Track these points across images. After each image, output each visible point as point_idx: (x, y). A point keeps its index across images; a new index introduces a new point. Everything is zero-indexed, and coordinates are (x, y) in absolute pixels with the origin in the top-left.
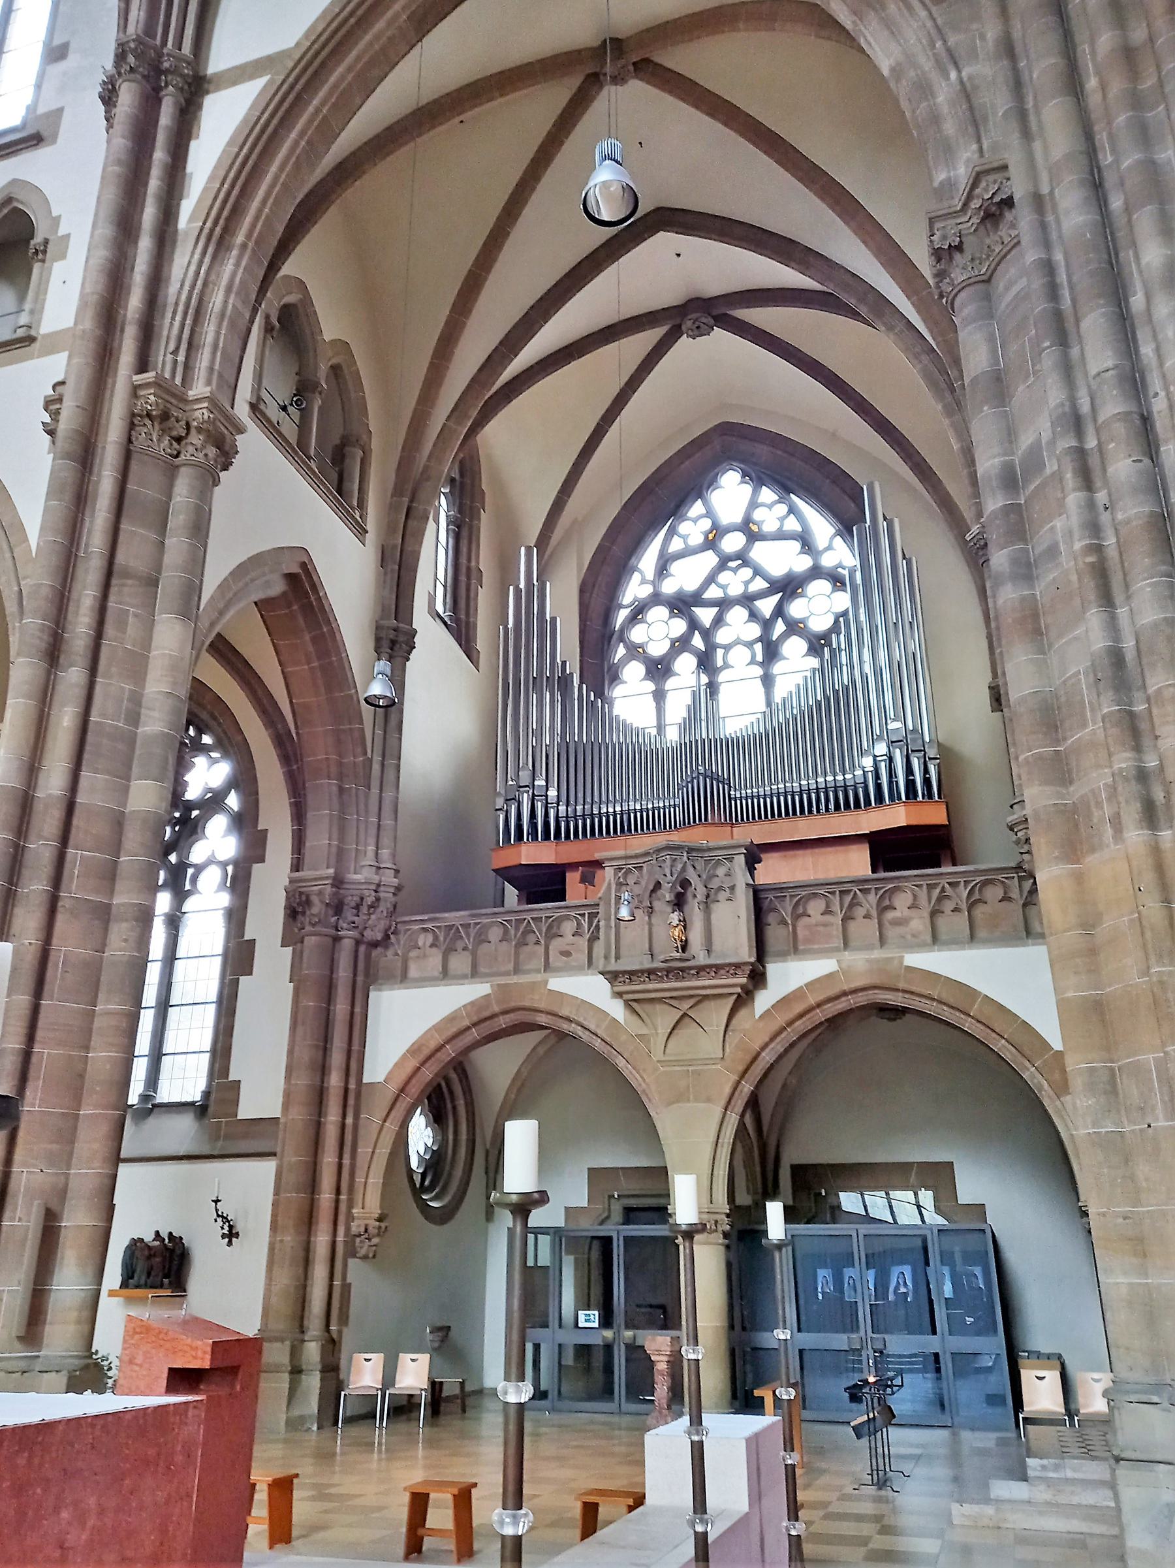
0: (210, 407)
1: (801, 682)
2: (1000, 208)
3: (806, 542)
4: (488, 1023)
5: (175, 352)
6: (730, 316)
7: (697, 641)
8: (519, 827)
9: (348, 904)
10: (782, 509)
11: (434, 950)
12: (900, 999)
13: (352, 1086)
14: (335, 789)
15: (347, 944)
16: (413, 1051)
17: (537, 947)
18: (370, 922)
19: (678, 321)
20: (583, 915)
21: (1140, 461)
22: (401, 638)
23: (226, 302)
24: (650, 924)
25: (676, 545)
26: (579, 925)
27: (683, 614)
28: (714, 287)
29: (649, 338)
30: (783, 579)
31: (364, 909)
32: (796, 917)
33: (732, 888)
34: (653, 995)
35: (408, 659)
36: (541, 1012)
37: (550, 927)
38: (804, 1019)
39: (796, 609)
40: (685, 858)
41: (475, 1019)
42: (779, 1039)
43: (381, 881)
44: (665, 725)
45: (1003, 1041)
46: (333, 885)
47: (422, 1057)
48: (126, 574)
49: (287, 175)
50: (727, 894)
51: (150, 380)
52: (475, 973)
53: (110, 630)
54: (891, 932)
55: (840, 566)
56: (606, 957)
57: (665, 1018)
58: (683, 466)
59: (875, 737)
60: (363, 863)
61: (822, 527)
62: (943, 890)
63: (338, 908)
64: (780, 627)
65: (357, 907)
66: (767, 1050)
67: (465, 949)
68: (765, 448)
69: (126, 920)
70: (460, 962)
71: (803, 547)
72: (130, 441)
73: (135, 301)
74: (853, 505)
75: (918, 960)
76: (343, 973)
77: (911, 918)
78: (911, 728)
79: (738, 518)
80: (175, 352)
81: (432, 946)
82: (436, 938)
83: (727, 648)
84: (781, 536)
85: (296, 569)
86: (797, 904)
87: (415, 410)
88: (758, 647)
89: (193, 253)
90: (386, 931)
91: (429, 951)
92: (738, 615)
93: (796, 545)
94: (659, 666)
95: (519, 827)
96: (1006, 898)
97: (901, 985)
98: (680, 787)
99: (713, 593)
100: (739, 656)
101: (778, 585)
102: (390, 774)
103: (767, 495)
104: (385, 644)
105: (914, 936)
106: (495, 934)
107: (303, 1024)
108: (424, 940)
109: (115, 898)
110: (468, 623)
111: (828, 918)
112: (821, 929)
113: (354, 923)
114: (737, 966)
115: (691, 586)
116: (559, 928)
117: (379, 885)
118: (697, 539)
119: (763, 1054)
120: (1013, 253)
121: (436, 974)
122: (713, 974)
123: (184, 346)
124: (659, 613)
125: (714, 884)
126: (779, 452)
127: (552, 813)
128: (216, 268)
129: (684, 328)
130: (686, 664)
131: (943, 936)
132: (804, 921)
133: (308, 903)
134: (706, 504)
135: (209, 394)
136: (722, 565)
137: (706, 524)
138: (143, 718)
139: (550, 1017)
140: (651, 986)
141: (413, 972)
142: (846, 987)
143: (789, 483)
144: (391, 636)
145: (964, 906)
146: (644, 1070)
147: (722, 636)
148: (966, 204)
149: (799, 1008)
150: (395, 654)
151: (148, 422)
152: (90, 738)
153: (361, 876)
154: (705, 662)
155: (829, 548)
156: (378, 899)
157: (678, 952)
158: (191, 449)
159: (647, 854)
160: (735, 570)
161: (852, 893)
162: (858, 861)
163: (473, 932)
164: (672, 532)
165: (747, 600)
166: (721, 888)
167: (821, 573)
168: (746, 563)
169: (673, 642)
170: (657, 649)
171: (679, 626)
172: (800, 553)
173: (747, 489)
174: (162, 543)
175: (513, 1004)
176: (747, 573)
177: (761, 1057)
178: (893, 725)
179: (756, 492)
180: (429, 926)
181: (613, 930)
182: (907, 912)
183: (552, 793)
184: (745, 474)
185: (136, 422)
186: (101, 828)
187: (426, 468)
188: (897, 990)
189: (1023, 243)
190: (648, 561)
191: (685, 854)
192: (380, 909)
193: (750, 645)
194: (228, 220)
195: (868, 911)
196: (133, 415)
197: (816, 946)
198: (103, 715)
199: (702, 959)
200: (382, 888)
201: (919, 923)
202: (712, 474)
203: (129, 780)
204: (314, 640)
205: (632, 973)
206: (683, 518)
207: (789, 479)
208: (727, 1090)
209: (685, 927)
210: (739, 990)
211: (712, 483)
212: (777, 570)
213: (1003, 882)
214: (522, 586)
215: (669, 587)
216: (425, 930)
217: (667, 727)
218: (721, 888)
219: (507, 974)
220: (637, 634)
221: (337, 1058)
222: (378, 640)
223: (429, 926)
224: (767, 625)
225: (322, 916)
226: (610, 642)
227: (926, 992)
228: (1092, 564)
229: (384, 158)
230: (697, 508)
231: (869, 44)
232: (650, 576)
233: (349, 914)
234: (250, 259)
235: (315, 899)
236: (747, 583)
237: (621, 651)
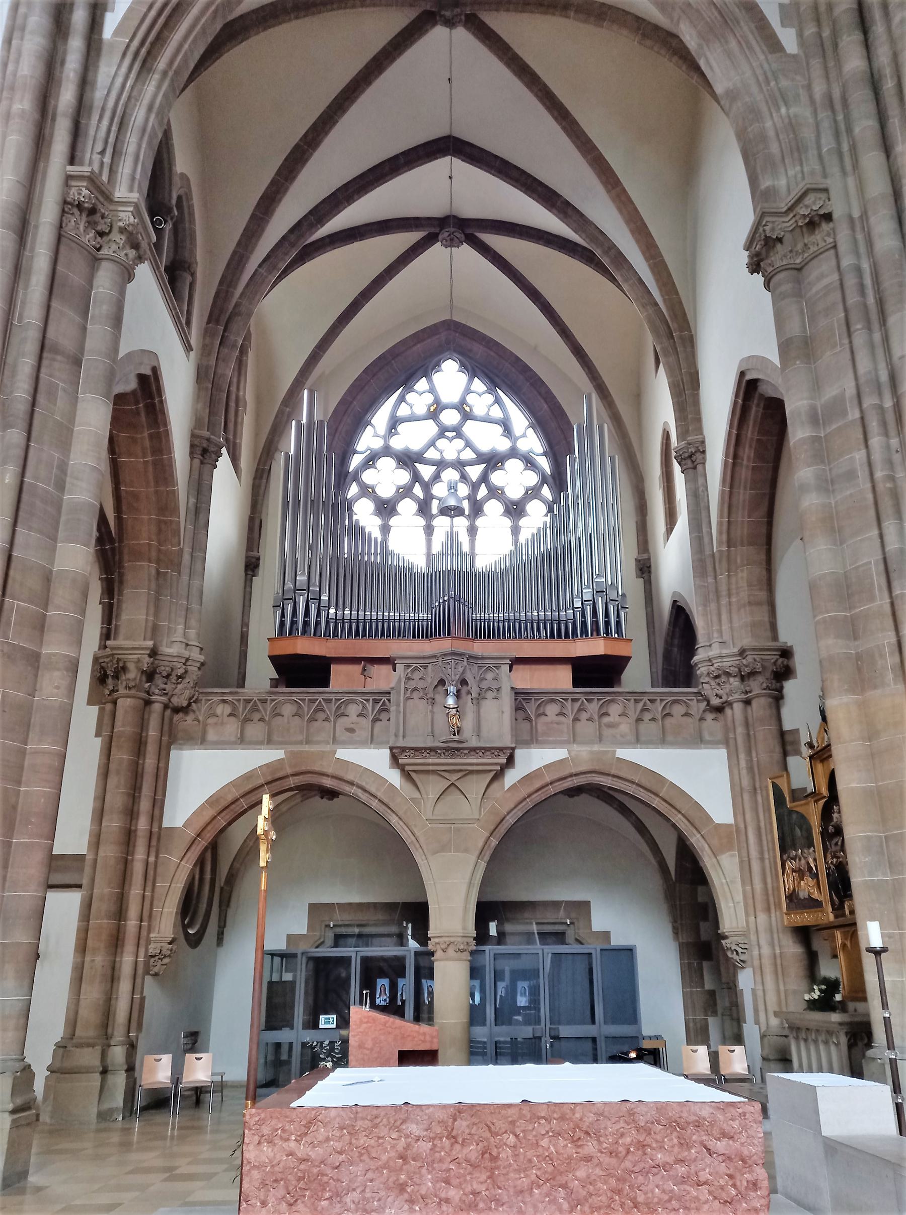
0: (134, 212)
1: (530, 537)
2: (820, 219)
3: (507, 430)
4: (278, 783)
5: (102, 153)
6: (476, 237)
7: (418, 490)
8: (293, 623)
9: (160, 673)
10: (490, 398)
11: (232, 719)
12: (609, 782)
13: (155, 830)
14: (153, 572)
15: (157, 707)
16: (211, 802)
17: (326, 723)
18: (176, 691)
19: (437, 230)
20: (566, 700)
22: (212, 449)
23: (147, 120)
24: (432, 712)
25: (404, 410)
26: (364, 707)
27: (408, 467)
28: (469, 210)
29: (414, 237)
30: (489, 453)
31: (173, 678)
32: (539, 716)
34: (431, 768)
35: (215, 467)
36: (328, 776)
37: (339, 707)
38: (540, 792)
39: (496, 478)
40: (465, 663)
41: (269, 778)
42: (520, 806)
43: (190, 656)
45: (680, 816)
46: (150, 656)
47: (220, 807)
48: (56, 350)
49: (206, 21)
50: (494, 694)
51: (86, 174)
52: (269, 741)
53: (42, 399)
54: (607, 732)
56: (396, 736)
57: (433, 787)
58: (415, 348)
59: (583, 587)
60: (174, 639)
61: (519, 420)
62: (645, 704)
63: (150, 675)
64: (483, 491)
65: (168, 676)
66: (510, 815)
67: (261, 720)
68: (481, 347)
69: (58, 670)
70: (254, 730)
71: (504, 431)
72: (61, 227)
73: (66, 96)
74: (546, 406)
75: (623, 753)
76: (153, 732)
77: (620, 723)
78: (610, 583)
79: (455, 399)
80: (102, 153)
81: (230, 715)
82: (235, 708)
84: (487, 420)
85: (148, 372)
86: (539, 705)
87: (235, 252)
89: (119, 66)
90: (191, 699)
91: (226, 719)
92: (450, 475)
93: (499, 429)
95: (293, 623)
96: (687, 714)
97: (613, 772)
99: (432, 454)
101: (484, 457)
102: (198, 566)
103: (478, 385)
104: (199, 451)
105: (622, 736)
106: (288, 710)
107: (118, 772)
108: (219, 710)
109: (44, 647)
111: (562, 718)
112: (555, 725)
113: (165, 690)
114: (501, 749)
115: (416, 446)
116: (345, 708)
117: (187, 660)
118: (421, 410)
119: (508, 817)
121: (233, 739)
122: (481, 754)
124: (386, 464)
125: (484, 685)
126: (492, 353)
127: (323, 614)
128: (139, 86)
129: (440, 237)
130: (407, 507)
131: (643, 739)
132: (543, 718)
133: (124, 669)
134: (430, 381)
135: (135, 200)
137: (430, 398)
138: (67, 486)
139: (334, 780)
140: (430, 761)
141: (211, 736)
142: (574, 771)
143: (497, 380)
144: (205, 445)
145: (659, 717)
146: (415, 826)
148: (791, 209)
149: (538, 785)
150: (205, 461)
151: (76, 211)
152: (25, 496)
153: (172, 649)
154: (424, 509)
155: (524, 435)
156: (186, 672)
157: (454, 735)
158: (114, 247)
159: (434, 657)
160: (451, 440)
161: (580, 702)
162: (563, 678)
163: (269, 707)
164: (402, 399)
165: (460, 465)
166: (489, 689)
167: (517, 454)
168: (459, 435)
169: (398, 488)
170: (386, 491)
173: (463, 378)
174: (84, 329)
175: (303, 768)
176: (459, 443)
177: (506, 819)
179: (471, 380)
180: (229, 698)
181: (402, 714)
182: (617, 719)
183: (325, 598)
184: (462, 365)
185: (66, 209)
186: (34, 583)
187: (237, 305)
188: (608, 775)
190: (381, 417)
191: (465, 660)
192: (187, 680)
194: (153, 44)
195: (591, 714)
196: (65, 202)
197: (551, 739)
198: (36, 478)
199: (474, 743)
200: (189, 663)
201: (625, 727)
202: (436, 359)
203: (55, 539)
204: (151, 437)
205: (417, 750)
206: (410, 389)
207: (497, 376)
208: (480, 844)
211: (437, 366)
212: (485, 447)
213: (685, 702)
214: (304, 421)
215: (397, 443)
216: (224, 701)
218: (489, 689)
219: (301, 743)
220: (368, 476)
221: (145, 805)
222: (192, 446)
223: (229, 698)
224: (475, 487)
225: (138, 681)
227: (629, 777)
228: (890, 489)
229: (265, 29)
230: (422, 384)
231: (711, 67)
233: (159, 681)
234: (169, 86)
235: (131, 666)
237: (354, 490)
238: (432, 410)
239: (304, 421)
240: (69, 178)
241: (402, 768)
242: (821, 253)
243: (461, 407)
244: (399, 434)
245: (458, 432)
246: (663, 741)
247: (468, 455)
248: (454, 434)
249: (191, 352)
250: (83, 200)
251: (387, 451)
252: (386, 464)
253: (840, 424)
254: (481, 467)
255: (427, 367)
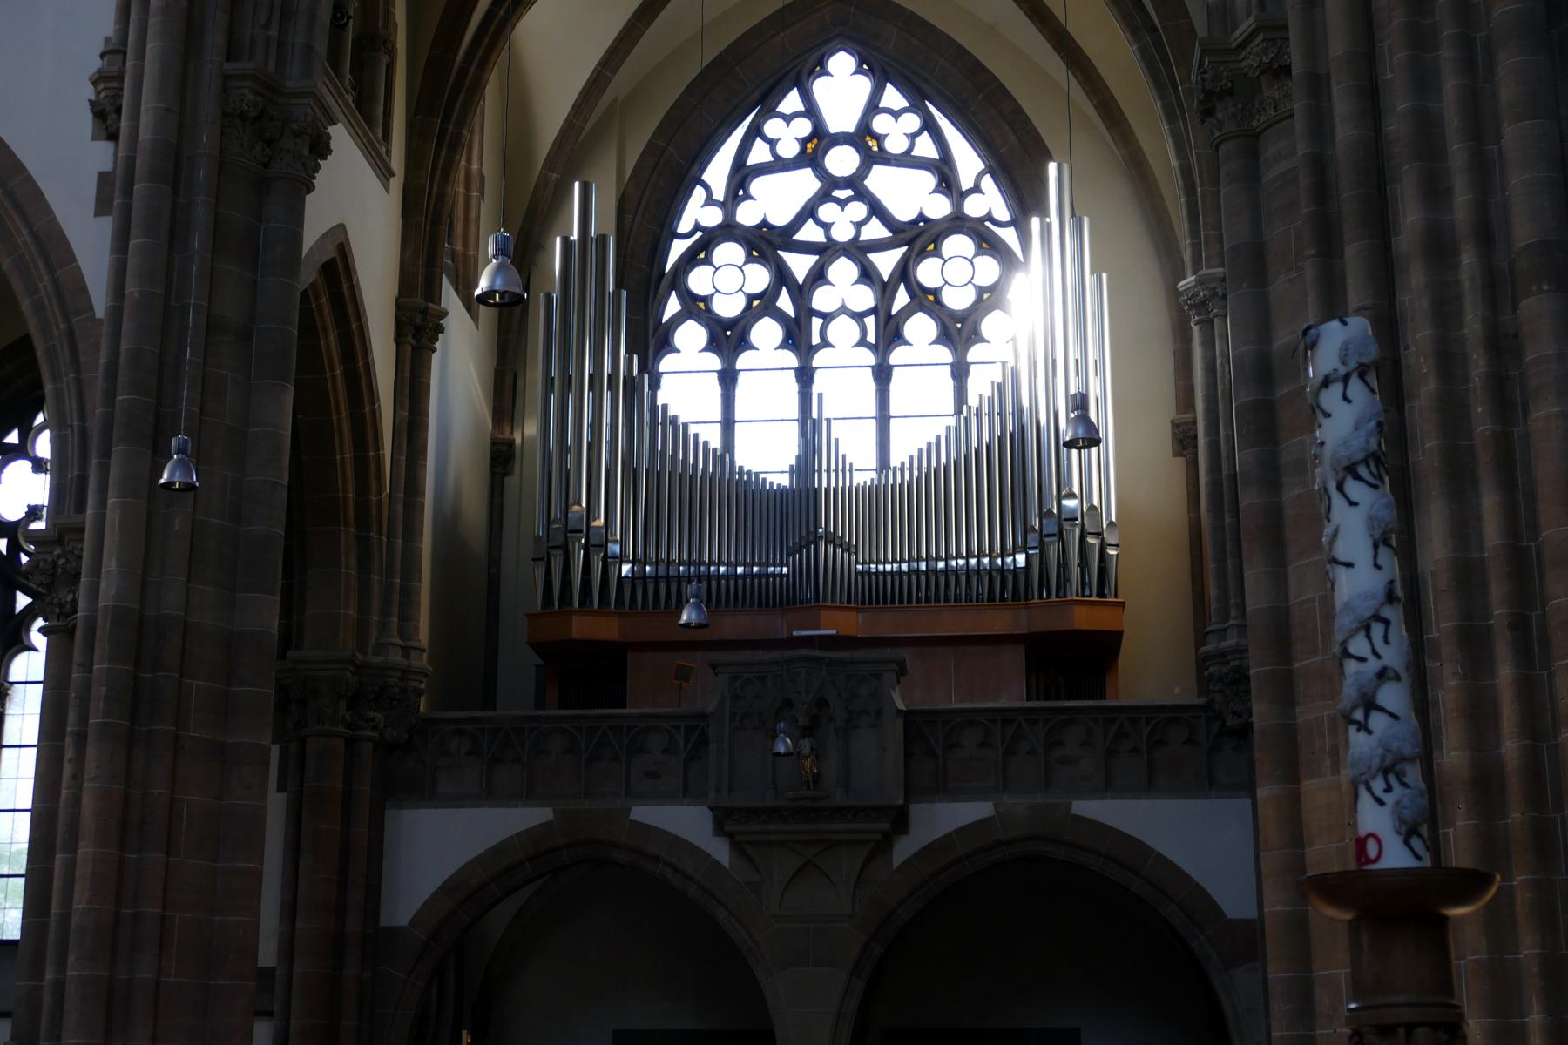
7: (785, 302)
10: (912, 122)
21: (1389, 411)
33: (879, 713)
39: (928, 272)
44: (734, 422)
52: (527, 795)
55: (989, 217)
61: (968, 161)
64: (902, 298)
71: (939, 185)
79: (850, 127)
83: (827, 317)
84: (907, 160)
88: (870, 321)
92: (843, 270)
93: (928, 179)
94: (729, 333)
98: (791, 550)
99: (810, 233)
100: (843, 332)
103: (893, 97)
110: (466, 257)
115: (780, 219)
118: (789, 150)
120: (1285, 122)
123: (276, 17)
124: (729, 252)
130: (766, 332)
136: (824, 196)
137: (804, 127)
143: (924, 86)
147: (822, 299)
154: (796, 337)
155: (976, 189)
160: (843, 203)
164: (755, 132)
165: (858, 250)
168: (862, 195)
169: (751, 298)
170: (728, 307)
171: (759, 277)
172: (934, 192)
173: (864, 85)
176: (858, 210)
178: (1070, 503)
184: (861, 61)
189: (1296, 116)
190: (717, 172)
193: (859, 317)
196: (225, 115)
206: (770, 112)
209: (817, 757)
210: (879, 837)
211: (819, 67)
212: (904, 213)
215: (747, 215)
217: (737, 425)
220: (699, 281)
226: (657, 288)
230: (792, 102)
232: (719, 195)
236: (859, 225)
237: (673, 306)
238: (809, 151)
239: (575, 237)
240: (227, 78)
241: (731, 836)
242: (1279, 121)
243: (863, 138)
244: (751, 198)
245: (855, 183)
246: (1149, 787)
247: (875, 230)
248: (849, 193)
249: (392, 180)
250: (246, 108)
251: (729, 230)
252: (729, 252)
253: (1290, 388)
254: (897, 254)
255: (800, 72)
